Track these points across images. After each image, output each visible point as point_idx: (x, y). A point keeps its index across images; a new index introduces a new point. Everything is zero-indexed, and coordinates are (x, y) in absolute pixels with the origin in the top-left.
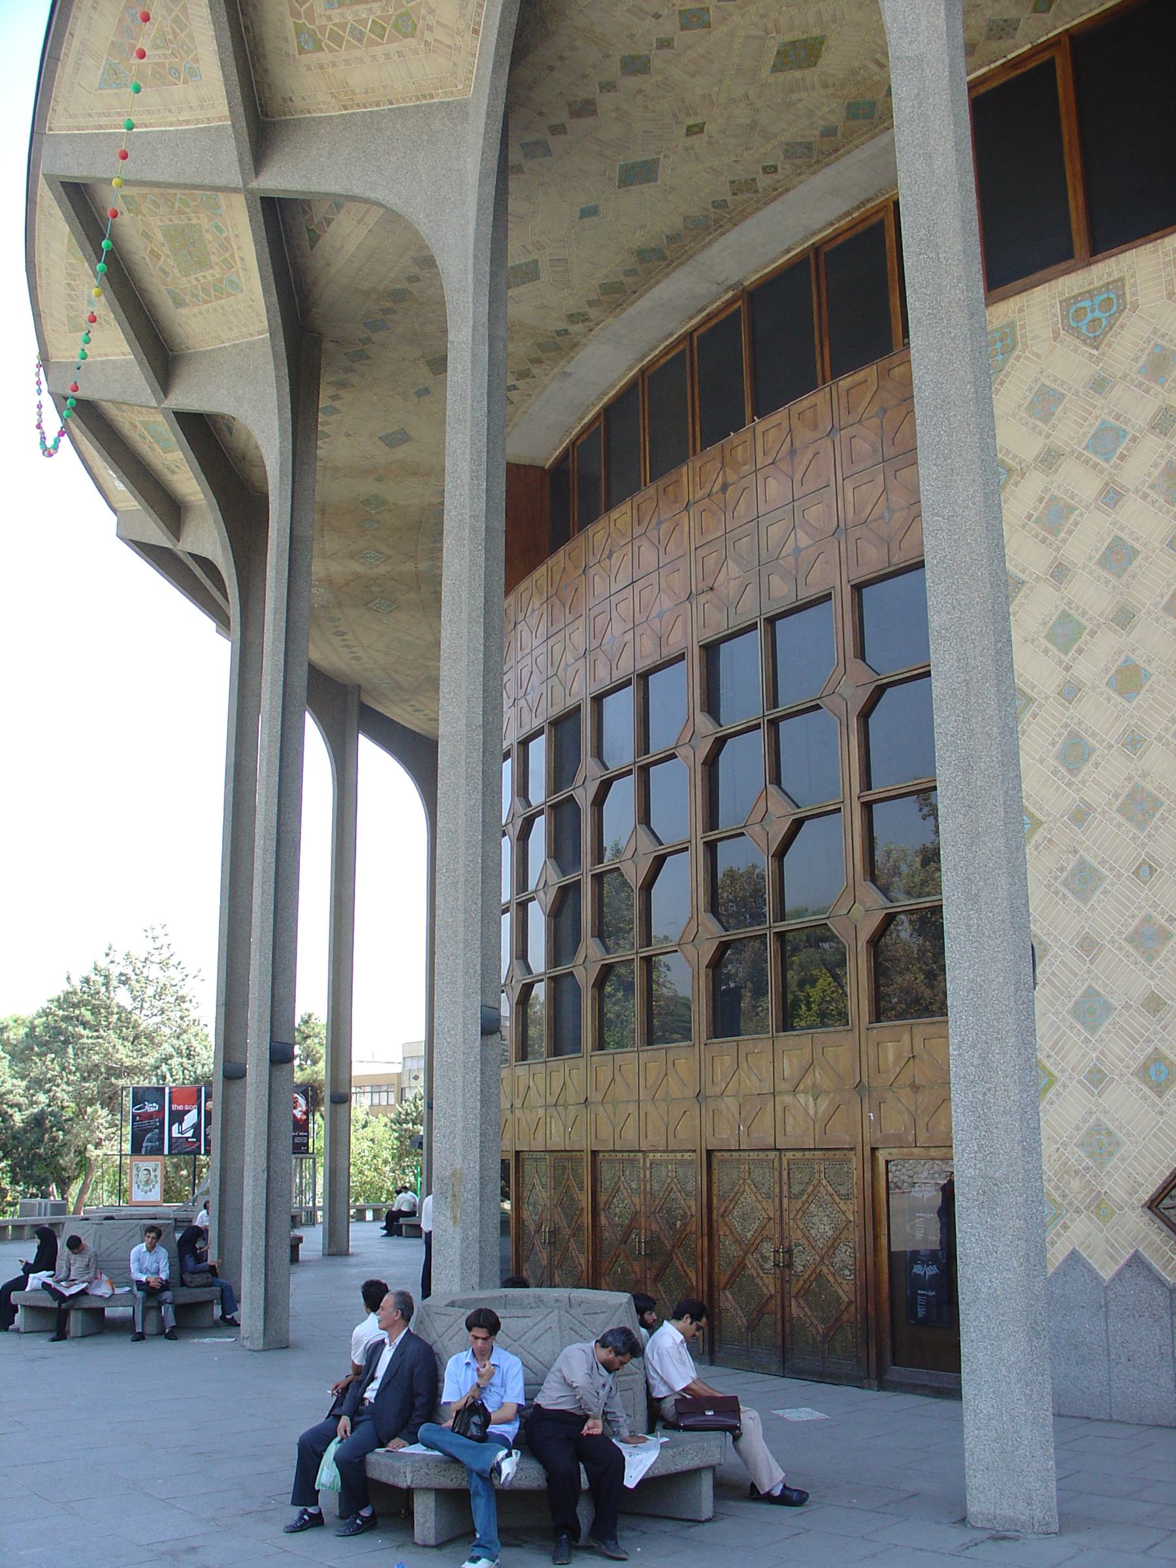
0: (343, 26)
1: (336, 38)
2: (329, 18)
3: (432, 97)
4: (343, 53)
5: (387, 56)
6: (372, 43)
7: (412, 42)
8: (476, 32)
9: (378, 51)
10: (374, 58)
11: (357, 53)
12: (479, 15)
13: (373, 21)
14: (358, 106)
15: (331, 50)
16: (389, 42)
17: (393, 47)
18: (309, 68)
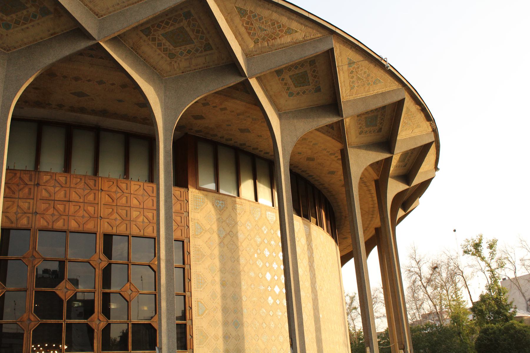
0: (159, 40)
1: (154, 39)
2: (159, 36)
3: (156, 69)
4: (150, 43)
5: (159, 54)
6: (160, 49)
7: (168, 59)
8: (183, 72)
9: (159, 51)
10: (156, 51)
11: (154, 46)
12: (188, 71)
13: (167, 48)
14: (136, 52)
15: (149, 39)
16: (164, 54)
17: (164, 55)
18: (137, 34)
